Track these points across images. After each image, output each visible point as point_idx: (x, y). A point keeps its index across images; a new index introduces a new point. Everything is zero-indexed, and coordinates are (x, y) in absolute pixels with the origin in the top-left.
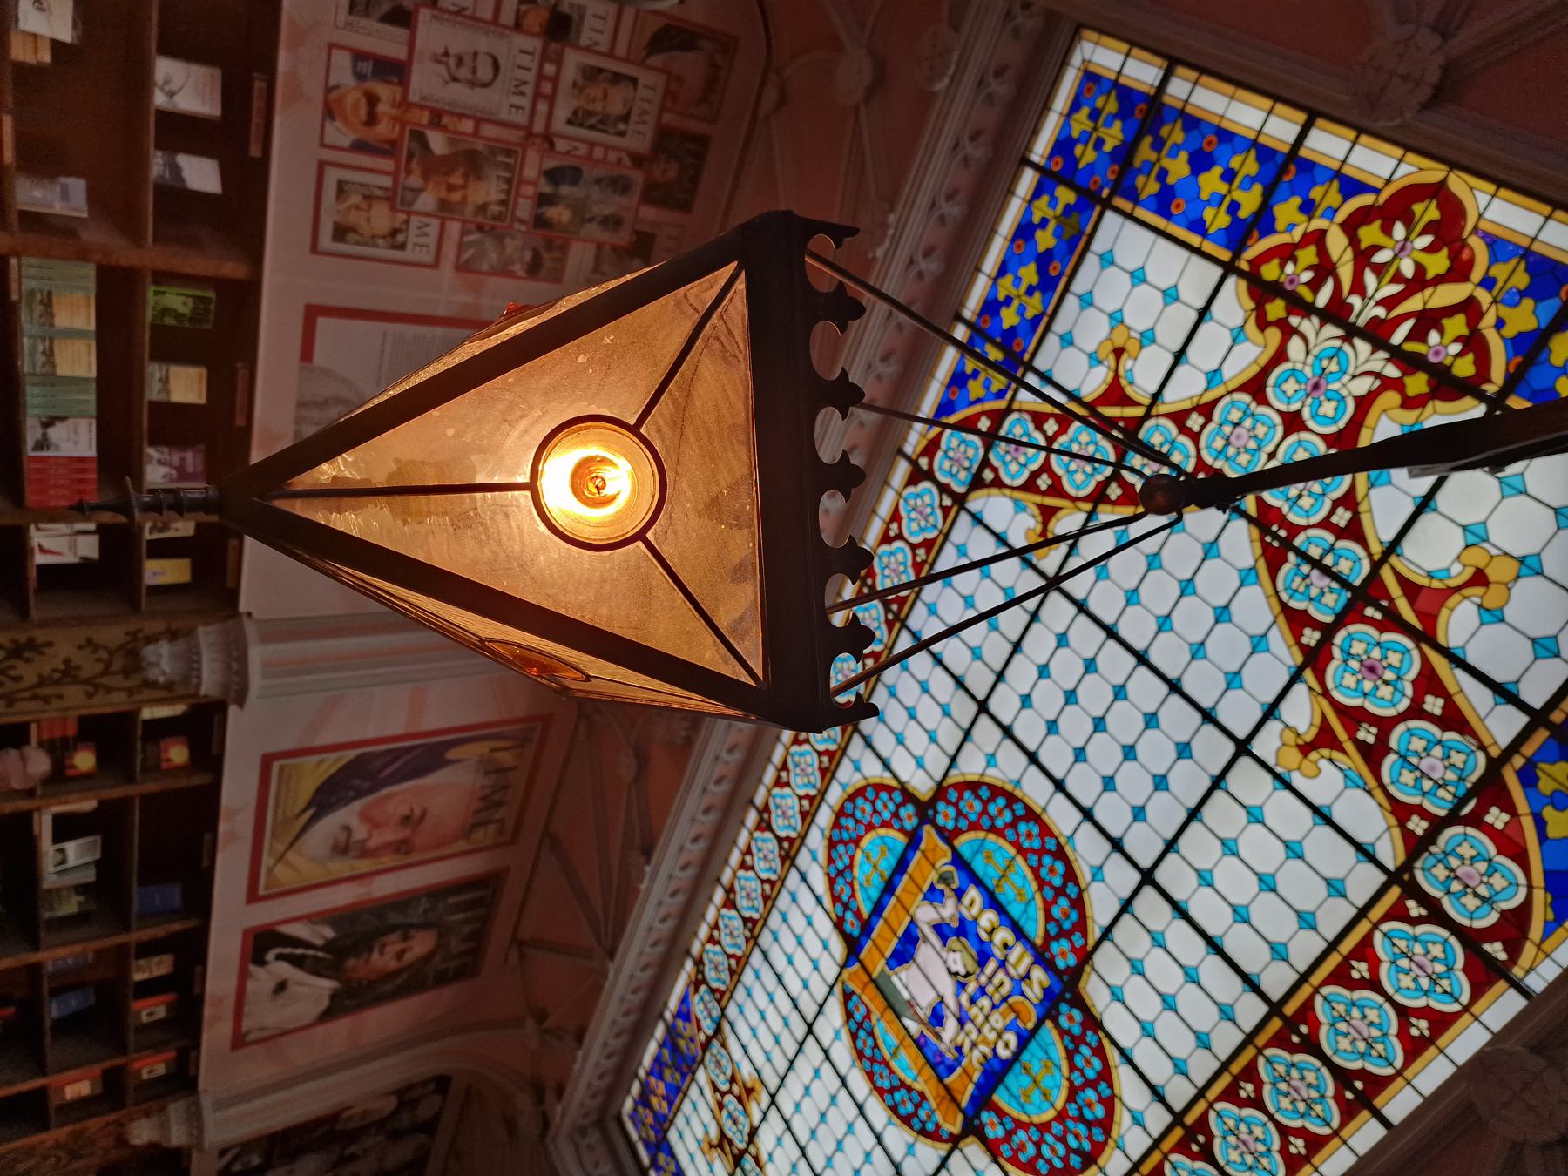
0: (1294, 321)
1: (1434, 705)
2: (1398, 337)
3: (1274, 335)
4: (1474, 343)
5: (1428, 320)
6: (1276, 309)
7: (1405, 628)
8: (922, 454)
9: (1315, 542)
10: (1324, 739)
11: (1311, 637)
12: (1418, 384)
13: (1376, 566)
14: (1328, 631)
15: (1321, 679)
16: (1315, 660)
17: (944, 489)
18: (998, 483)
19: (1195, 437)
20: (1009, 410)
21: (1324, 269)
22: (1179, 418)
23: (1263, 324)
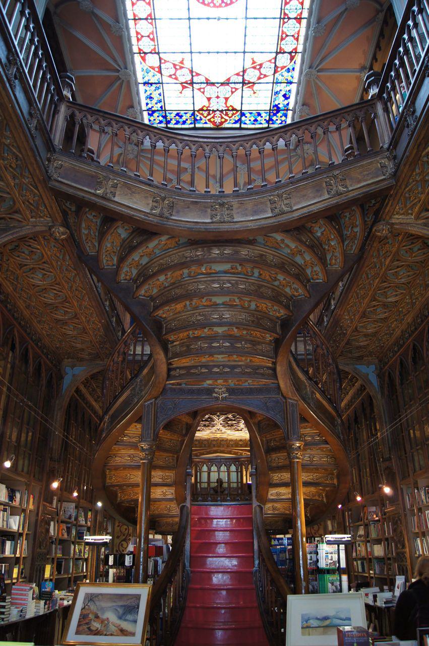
0: (226, 108)
1: (174, 77)
2: (211, 112)
3: (228, 105)
4: (202, 114)
5: (209, 114)
6: (230, 108)
7: (184, 83)
8: (295, 56)
9: (203, 86)
10: (182, 62)
11: (194, 74)
12: (205, 109)
13: (193, 88)
14: (193, 76)
15: (189, 69)
16: (191, 72)
17: (285, 52)
18: (270, 61)
19: (232, 88)
20: (274, 74)
21: (227, 115)
22: (236, 89)
23: (231, 106)
